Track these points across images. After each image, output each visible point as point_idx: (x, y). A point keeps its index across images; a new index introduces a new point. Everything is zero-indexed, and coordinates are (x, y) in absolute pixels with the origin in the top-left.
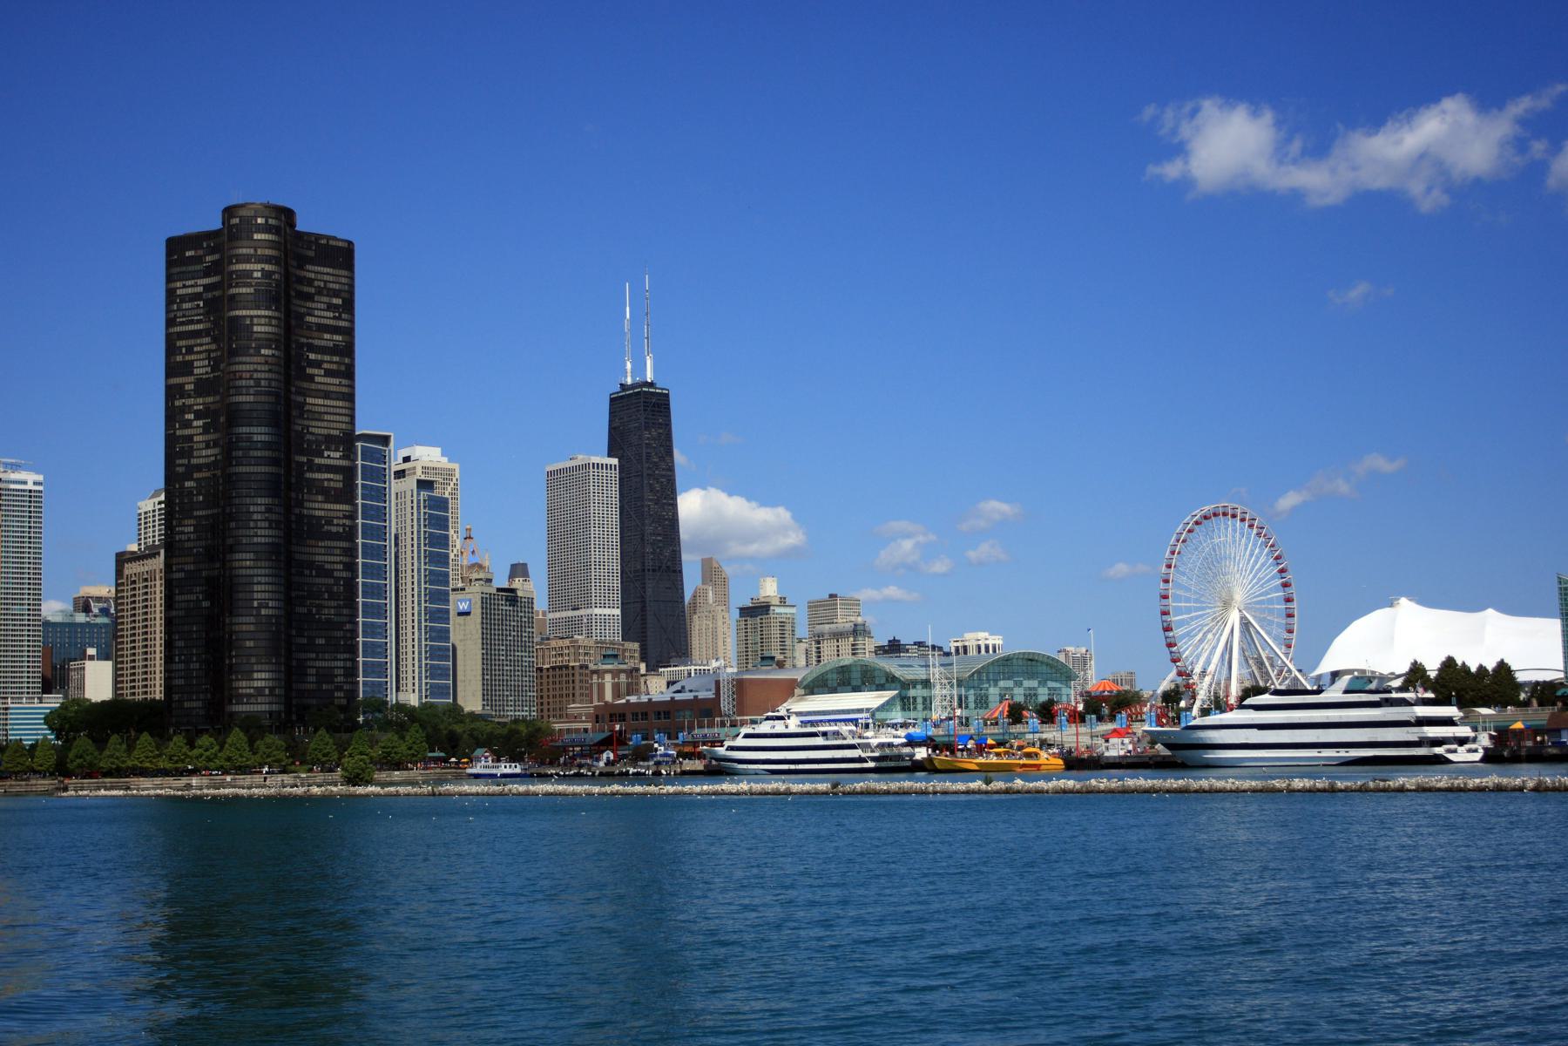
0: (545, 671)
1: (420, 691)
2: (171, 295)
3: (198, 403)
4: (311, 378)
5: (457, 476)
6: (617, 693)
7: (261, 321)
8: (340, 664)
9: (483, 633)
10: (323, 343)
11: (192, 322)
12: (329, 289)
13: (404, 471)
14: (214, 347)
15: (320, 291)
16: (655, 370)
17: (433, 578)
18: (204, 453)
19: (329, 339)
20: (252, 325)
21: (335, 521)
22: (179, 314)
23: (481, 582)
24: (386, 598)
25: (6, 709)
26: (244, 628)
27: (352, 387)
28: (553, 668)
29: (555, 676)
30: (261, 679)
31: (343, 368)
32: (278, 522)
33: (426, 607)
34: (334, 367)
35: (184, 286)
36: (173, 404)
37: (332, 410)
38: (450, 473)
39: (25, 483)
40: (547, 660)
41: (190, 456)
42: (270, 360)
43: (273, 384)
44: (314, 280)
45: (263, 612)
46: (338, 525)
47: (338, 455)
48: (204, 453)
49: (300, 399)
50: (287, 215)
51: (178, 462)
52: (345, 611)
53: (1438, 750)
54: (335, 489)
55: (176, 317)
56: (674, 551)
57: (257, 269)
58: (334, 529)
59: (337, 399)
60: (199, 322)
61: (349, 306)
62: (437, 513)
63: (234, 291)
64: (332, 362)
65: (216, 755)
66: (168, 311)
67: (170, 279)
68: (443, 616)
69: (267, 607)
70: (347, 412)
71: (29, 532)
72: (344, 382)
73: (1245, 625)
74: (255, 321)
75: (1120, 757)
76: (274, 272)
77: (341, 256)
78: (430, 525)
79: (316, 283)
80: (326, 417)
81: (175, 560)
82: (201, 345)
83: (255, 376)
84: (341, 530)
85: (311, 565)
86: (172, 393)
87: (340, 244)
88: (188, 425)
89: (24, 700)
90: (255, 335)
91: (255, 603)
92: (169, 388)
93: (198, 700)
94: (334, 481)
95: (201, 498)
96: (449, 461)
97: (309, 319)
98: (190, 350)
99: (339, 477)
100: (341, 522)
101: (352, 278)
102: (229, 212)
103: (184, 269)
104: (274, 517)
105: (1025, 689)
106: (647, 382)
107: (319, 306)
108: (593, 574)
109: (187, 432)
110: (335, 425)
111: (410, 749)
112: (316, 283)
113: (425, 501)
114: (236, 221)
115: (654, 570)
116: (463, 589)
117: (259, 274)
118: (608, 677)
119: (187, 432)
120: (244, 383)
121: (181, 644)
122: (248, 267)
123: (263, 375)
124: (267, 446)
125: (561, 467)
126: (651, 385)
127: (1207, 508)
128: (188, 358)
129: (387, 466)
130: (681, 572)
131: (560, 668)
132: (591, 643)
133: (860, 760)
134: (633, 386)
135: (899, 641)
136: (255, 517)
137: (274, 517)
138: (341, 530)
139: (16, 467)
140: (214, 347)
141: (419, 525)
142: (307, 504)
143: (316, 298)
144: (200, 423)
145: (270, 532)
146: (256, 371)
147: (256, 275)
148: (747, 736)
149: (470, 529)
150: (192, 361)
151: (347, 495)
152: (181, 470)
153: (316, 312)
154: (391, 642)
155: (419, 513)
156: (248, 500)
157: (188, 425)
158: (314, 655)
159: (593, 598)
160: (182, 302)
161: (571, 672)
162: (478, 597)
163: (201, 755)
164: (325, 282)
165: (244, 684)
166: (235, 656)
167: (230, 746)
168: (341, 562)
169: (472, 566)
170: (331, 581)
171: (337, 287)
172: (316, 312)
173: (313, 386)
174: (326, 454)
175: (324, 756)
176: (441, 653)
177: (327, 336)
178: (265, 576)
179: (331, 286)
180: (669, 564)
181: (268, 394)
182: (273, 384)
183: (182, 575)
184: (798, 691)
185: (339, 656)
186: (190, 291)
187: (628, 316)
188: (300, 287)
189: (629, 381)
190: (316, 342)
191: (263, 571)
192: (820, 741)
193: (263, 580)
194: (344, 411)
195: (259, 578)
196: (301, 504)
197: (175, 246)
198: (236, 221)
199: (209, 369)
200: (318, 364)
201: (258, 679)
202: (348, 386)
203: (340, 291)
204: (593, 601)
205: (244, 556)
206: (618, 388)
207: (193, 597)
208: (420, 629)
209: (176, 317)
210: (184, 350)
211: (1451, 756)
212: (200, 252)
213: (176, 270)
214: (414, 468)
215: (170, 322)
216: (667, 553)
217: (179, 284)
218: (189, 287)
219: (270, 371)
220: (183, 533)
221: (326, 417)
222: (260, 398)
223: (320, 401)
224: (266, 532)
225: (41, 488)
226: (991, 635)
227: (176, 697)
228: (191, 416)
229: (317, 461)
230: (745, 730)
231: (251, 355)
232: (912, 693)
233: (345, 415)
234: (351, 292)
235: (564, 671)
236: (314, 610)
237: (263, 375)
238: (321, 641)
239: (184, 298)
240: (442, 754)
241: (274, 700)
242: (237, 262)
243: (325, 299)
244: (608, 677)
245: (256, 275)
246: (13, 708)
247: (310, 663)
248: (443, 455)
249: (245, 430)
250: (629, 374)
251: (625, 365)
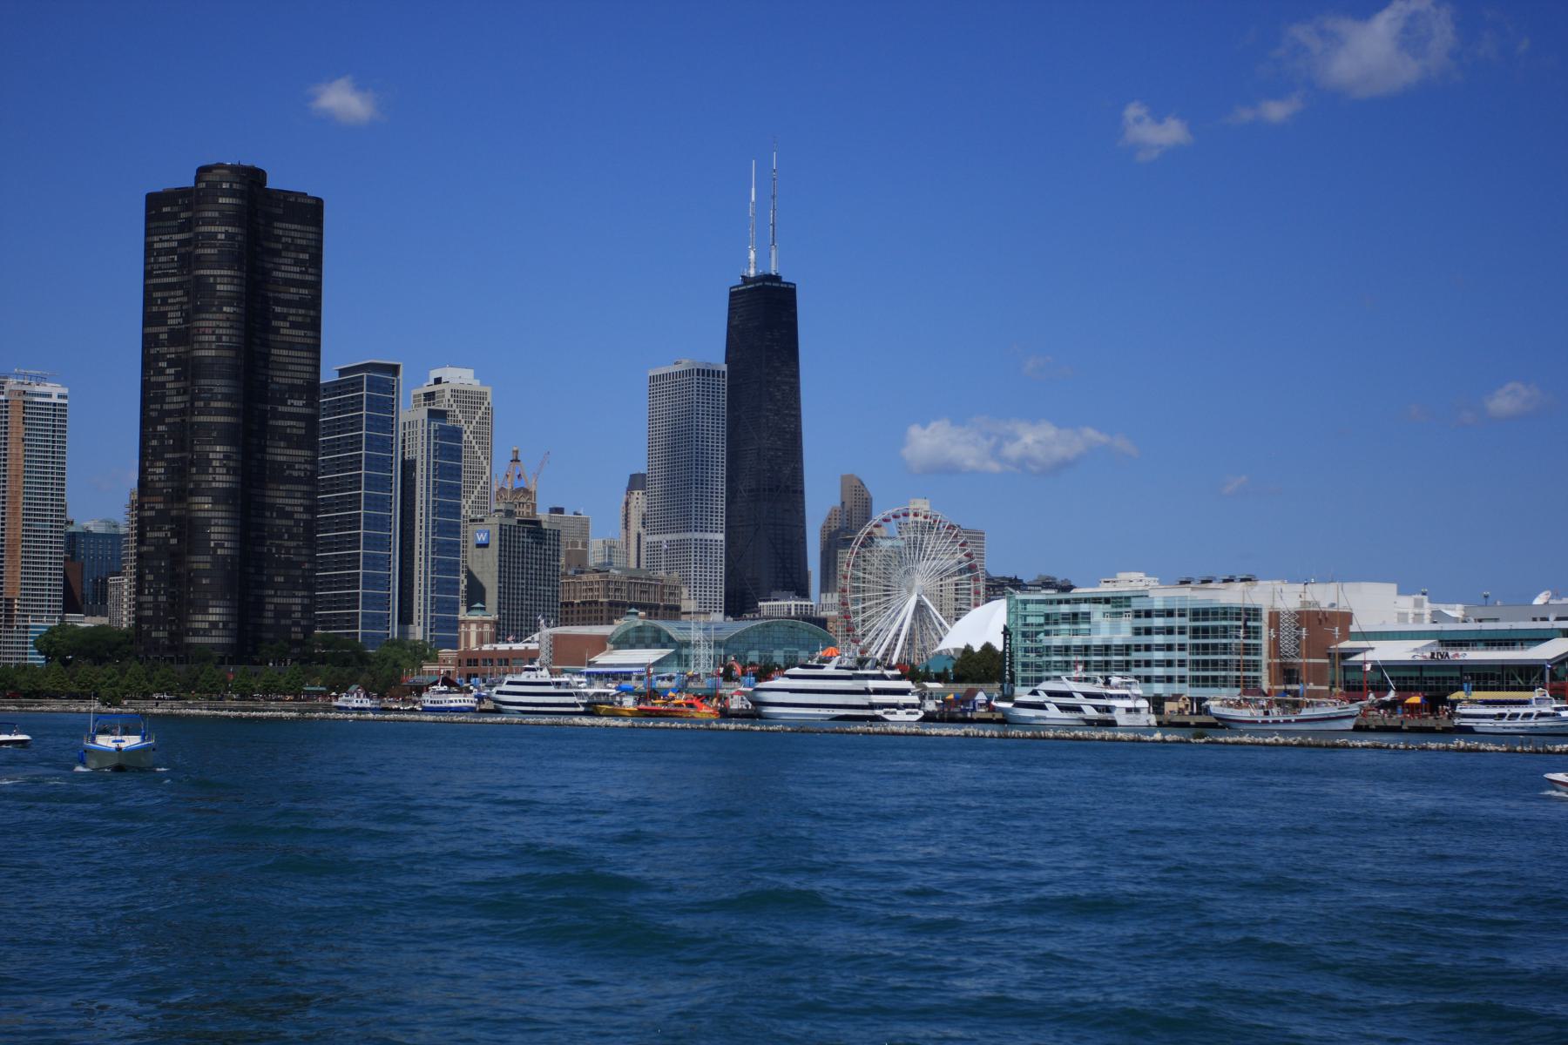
0: (575, 606)
1: (425, 624)
2: (148, 247)
3: (171, 352)
4: (277, 330)
5: (489, 399)
6: (481, 641)
7: (223, 280)
8: (298, 601)
9: (500, 566)
10: (288, 297)
11: (167, 275)
12: (296, 245)
13: (433, 393)
14: (185, 299)
15: (287, 247)
17: (442, 510)
18: (175, 399)
19: (294, 293)
20: (216, 284)
21: (297, 466)
22: (156, 266)
23: (503, 514)
24: (390, 530)
25: (27, 627)
26: (201, 566)
27: (318, 339)
28: (584, 603)
29: (584, 612)
30: (216, 614)
31: (308, 320)
32: (235, 469)
33: (433, 540)
34: (300, 319)
35: (161, 241)
36: (148, 352)
37: (296, 361)
38: (481, 397)
39: (50, 396)
40: (578, 594)
41: (163, 402)
42: (231, 317)
43: (234, 339)
44: (281, 236)
45: (219, 552)
46: (299, 470)
47: (301, 403)
48: (175, 399)
50: (252, 178)
51: (152, 407)
52: (304, 551)
53: (878, 712)
54: (297, 435)
55: (153, 270)
56: (794, 468)
57: (221, 231)
58: (295, 474)
59: (301, 350)
60: (173, 275)
61: (316, 260)
62: (448, 441)
63: (199, 251)
64: (297, 314)
65: (118, 682)
66: (146, 264)
67: (148, 233)
68: (454, 548)
69: (222, 547)
70: (311, 362)
71: (53, 447)
72: (309, 333)
73: (920, 608)
74: (219, 280)
75: (739, 710)
76: (237, 234)
77: (310, 211)
78: (441, 456)
79: (284, 240)
80: (290, 367)
81: (146, 499)
82: (175, 297)
83: (217, 332)
84: (302, 475)
85: (272, 507)
86: (148, 341)
87: (309, 201)
88: (161, 372)
89: (45, 619)
90: (218, 294)
91: (212, 544)
92: (145, 337)
93: (164, 630)
94: (296, 428)
95: (171, 442)
96: (482, 384)
97: (275, 274)
98: (164, 301)
99: (302, 424)
100: (303, 467)
101: (321, 234)
102: (203, 171)
103: (161, 224)
104: (232, 464)
105: (786, 652)
106: (771, 275)
107: (286, 261)
108: (694, 494)
109: (161, 379)
110: (298, 375)
111: (288, 683)
112: (284, 240)
113: (436, 431)
114: (202, 185)
115: (770, 490)
117: (223, 236)
118: (473, 627)
119: (161, 379)
120: (206, 338)
121: (150, 577)
122: (213, 229)
123: (224, 331)
124: (226, 397)
125: (664, 372)
127: (890, 511)
128: (163, 309)
129: (395, 396)
130: (802, 492)
131: (590, 603)
132: (624, 579)
133: (575, 705)
135: (1021, 581)
136: (215, 463)
137: (232, 464)
138: (302, 475)
139: (41, 379)
140: (185, 299)
141: (429, 456)
142: (270, 450)
143: (284, 254)
144: (172, 371)
145: (228, 478)
146: (218, 327)
147: (220, 236)
148: (509, 683)
149: (517, 452)
150: (166, 312)
151: (309, 441)
152: (154, 414)
153: (283, 268)
154: (394, 574)
155: (429, 443)
156: (208, 448)
157: (161, 372)
158: (273, 592)
159: (693, 521)
160: (159, 255)
162: (497, 529)
163: (105, 683)
164: (293, 238)
165: (200, 617)
166: (194, 592)
167: (130, 675)
168: (301, 505)
169: (519, 490)
170: (292, 523)
171: (304, 242)
172: (283, 268)
173: (279, 338)
174: (289, 402)
175: (211, 686)
176: (449, 586)
177: (293, 290)
178: (222, 518)
179: (299, 242)
180: (789, 483)
181: (229, 348)
182: (234, 339)
183: (153, 513)
184: (609, 646)
185: (297, 593)
186: (166, 245)
187: (753, 199)
188: (265, 244)
189: (752, 273)
190: (282, 296)
191: (223, 514)
192: (552, 689)
193: (220, 522)
194: (308, 362)
195: (216, 521)
196: (263, 450)
197: (155, 202)
198: (202, 185)
199: (181, 320)
200: (284, 317)
201: (212, 614)
202: (315, 338)
203: (307, 246)
204: (693, 524)
205: (203, 499)
206: (739, 281)
207: (162, 534)
208: (426, 561)
209: (153, 270)
210: (159, 302)
211: (887, 717)
212: (176, 209)
213: (153, 225)
214: (443, 391)
215: (148, 274)
217: (156, 238)
218: (164, 241)
219: (231, 327)
220: (154, 473)
221: (290, 367)
222: (221, 353)
223: (285, 352)
224: (224, 478)
225: (65, 401)
226: (1147, 576)
227: (145, 627)
228: (164, 364)
229: (280, 409)
230: (508, 678)
231: (214, 312)
232: (684, 651)
233: (309, 365)
234: (320, 249)
235: (570, 609)
236: (274, 551)
237: (224, 331)
238: (281, 579)
239: (160, 252)
240: (324, 689)
241: (227, 633)
242: (203, 225)
243: (293, 255)
244: (473, 627)
245: (220, 236)
246: (33, 627)
247: (267, 600)
248: (475, 378)
249: (207, 382)
250: (752, 265)
251: (749, 255)
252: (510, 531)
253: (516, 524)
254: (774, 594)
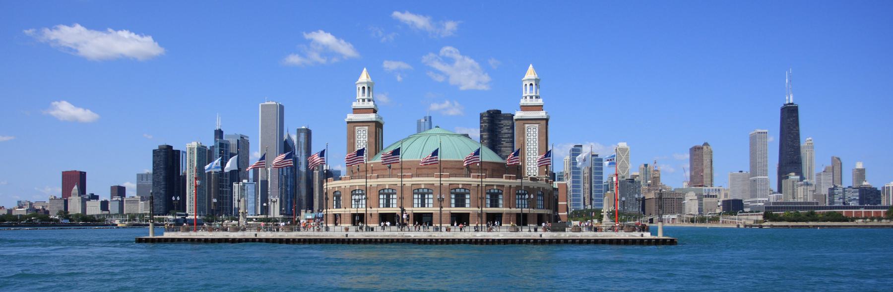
4: (503, 144)
16: (794, 99)
38: (627, 149)
49: (500, 149)
126: (792, 104)
130: (801, 163)
200: (504, 141)
216: (795, 157)
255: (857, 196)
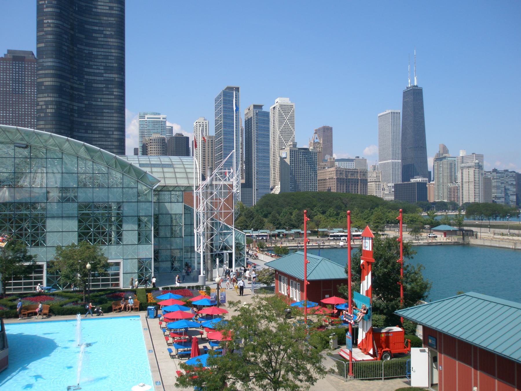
4: (96, 39)
16: (418, 82)
28: (329, 179)
38: (292, 106)
39: (160, 118)
96: (291, 102)
116: (284, 149)
126: (417, 86)
131: (331, 178)
134: (410, 87)
161: (334, 180)
252: (295, 152)
253: (297, 150)
254: (415, 177)
255: (513, 181)
